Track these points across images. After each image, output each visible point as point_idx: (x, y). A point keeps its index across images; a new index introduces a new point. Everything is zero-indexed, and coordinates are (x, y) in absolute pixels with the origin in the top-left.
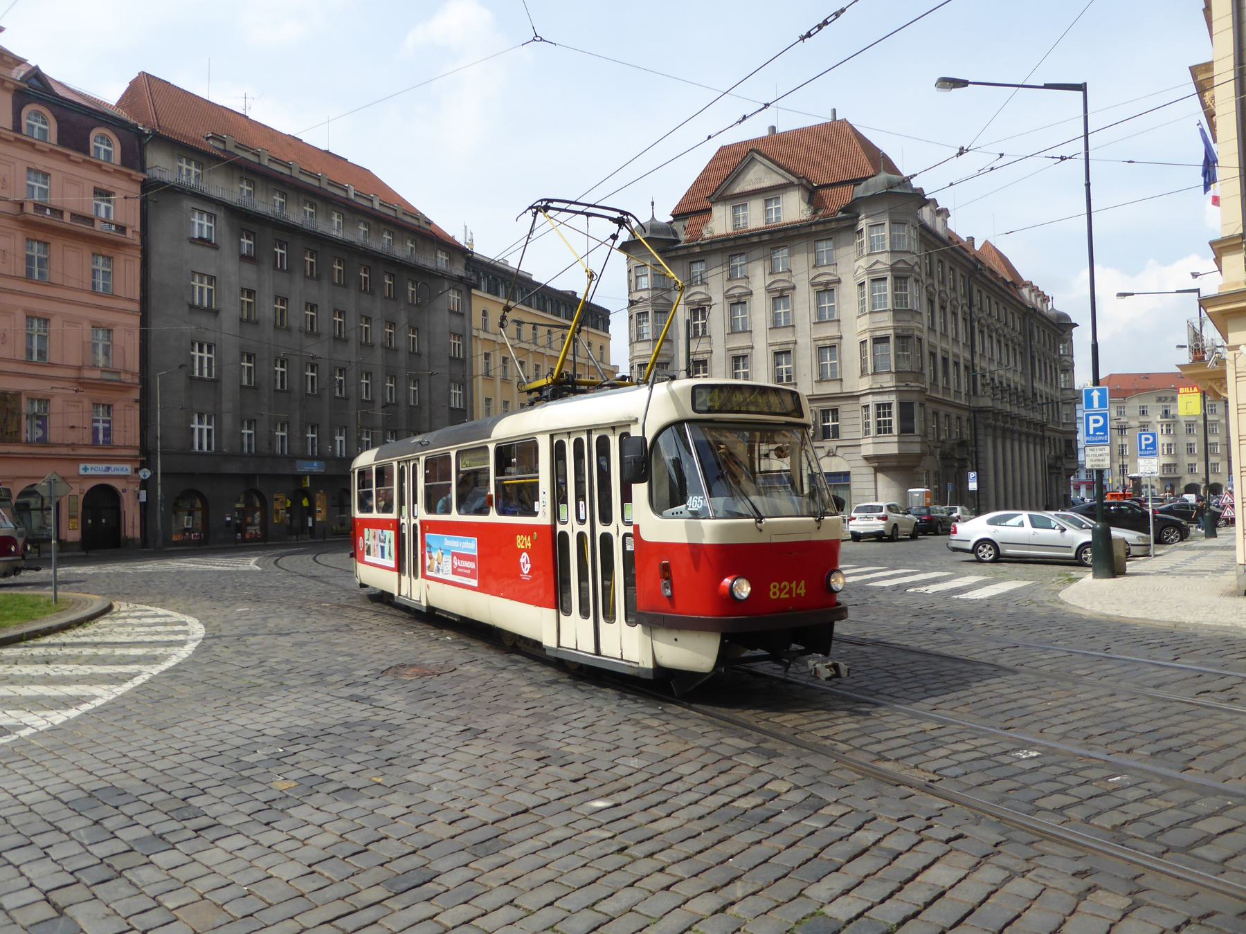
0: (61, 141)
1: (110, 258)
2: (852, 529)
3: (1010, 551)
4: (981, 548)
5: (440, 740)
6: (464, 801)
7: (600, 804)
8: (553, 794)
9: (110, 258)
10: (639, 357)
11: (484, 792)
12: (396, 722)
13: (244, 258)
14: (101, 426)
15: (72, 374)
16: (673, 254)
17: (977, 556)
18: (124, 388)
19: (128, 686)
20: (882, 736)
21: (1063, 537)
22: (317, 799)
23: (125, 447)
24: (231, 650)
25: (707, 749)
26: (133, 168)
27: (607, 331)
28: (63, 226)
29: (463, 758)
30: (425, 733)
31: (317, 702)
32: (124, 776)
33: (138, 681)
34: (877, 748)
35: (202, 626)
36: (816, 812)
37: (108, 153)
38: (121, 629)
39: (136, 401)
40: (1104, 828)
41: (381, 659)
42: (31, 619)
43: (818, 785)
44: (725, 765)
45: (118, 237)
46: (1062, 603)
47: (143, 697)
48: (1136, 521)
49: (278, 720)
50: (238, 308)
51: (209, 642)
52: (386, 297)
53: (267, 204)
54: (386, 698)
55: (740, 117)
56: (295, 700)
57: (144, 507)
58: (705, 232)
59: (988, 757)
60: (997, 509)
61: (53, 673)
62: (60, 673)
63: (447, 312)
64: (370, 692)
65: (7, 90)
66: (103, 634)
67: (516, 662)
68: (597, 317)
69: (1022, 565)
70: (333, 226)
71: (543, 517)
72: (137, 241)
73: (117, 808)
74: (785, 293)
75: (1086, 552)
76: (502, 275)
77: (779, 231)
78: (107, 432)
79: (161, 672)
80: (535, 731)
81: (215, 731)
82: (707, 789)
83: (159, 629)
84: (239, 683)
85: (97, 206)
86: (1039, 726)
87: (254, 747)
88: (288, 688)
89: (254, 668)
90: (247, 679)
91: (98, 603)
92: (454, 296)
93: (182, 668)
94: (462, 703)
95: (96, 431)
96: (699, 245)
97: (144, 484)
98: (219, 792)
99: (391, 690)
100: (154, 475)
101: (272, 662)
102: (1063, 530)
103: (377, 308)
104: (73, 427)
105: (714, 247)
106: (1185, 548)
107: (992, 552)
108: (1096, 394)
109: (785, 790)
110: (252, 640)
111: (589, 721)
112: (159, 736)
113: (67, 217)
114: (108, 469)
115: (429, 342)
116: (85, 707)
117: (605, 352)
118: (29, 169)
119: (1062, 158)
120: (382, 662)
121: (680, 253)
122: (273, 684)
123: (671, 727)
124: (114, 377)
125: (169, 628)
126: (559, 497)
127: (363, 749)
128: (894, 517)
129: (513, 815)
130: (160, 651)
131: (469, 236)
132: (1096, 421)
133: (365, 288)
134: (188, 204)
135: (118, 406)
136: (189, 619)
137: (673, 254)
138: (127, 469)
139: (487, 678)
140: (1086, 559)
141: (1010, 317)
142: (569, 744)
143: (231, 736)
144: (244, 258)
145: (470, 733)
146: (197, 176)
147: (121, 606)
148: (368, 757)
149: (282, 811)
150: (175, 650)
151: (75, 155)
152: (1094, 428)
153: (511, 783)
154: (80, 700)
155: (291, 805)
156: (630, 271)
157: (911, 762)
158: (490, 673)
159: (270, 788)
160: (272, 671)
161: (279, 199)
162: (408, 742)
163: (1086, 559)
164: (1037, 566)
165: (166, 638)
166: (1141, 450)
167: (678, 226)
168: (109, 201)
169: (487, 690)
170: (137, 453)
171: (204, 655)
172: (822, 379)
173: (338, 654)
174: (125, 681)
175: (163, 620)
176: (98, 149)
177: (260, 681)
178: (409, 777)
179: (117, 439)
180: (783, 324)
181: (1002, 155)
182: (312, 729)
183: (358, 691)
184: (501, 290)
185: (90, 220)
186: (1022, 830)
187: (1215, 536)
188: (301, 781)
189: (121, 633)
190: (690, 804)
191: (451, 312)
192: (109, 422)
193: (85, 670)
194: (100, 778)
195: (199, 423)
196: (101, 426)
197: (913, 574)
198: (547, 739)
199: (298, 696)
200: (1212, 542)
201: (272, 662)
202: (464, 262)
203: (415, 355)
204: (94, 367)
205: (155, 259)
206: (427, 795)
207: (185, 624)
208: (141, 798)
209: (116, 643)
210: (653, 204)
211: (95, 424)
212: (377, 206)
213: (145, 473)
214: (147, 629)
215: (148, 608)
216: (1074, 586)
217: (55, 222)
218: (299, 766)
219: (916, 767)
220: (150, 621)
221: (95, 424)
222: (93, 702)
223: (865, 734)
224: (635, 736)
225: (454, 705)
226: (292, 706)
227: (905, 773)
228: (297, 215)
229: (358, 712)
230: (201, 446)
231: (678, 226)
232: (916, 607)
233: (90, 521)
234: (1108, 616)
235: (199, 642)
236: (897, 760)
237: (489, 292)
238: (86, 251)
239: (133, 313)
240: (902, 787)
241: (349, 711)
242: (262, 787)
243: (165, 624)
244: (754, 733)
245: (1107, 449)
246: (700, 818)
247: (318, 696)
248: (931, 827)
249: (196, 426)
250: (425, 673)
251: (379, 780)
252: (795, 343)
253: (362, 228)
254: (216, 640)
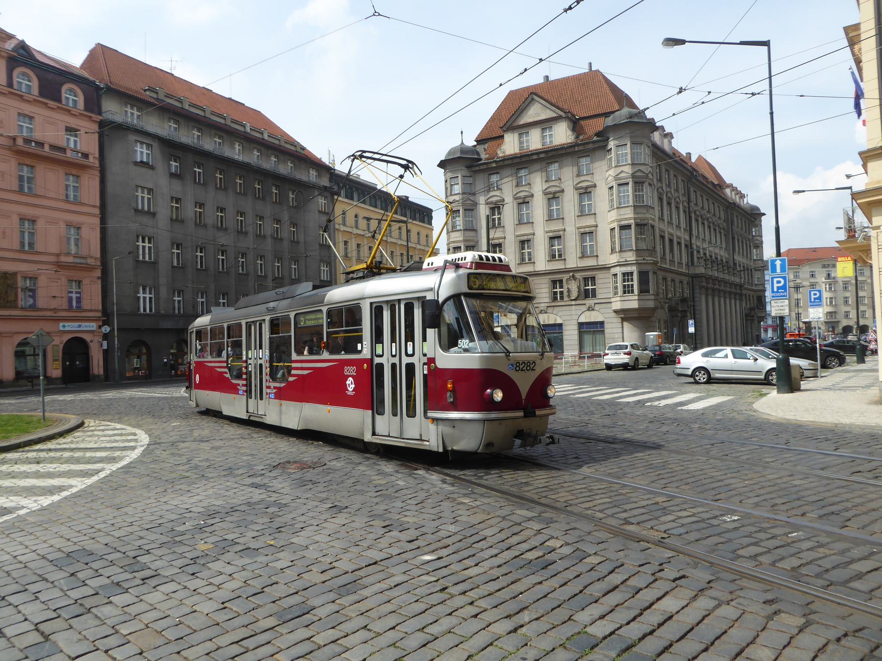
0: (41, 94)
1: (78, 177)
2: (606, 361)
3: (718, 375)
4: (697, 373)
5: (315, 514)
6: (332, 557)
7: (427, 558)
8: (394, 551)
9: (78, 177)
10: (454, 242)
11: (346, 550)
12: (283, 502)
13: (173, 175)
14: (74, 296)
15: (52, 259)
16: (477, 168)
17: (695, 379)
18: (90, 268)
19: (95, 478)
20: (627, 507)
21: (756, 364)
22: (228, 557)
23: (91, 311)
24: (167, 452)
25: (504, 518)
26: (92, 112)
27: (431, 225)
28: (44, 154)
29: (331, 526)
30: (304, 509)
31: (227, 489)
32: (92, 541)
33: (102, 475)
34: (624, 515)
35: (147, 436)
36: (581, 561)
37: (75, 102)
38: (90, 439)
39: (99, 278)
40: (786, 569)
41: (272, 458)
42: (27, 432)
43: (583, 542)
44: (517, 529)
45: (84, 161)
46: (755, 411)
47: (105, 486)
48: (808, 352)
49: (201, 501)
50: (169, 211)
51: (152, 447)
52: (273, 202)
53: (188, 136)
54: (276, 484)
55: (522, 70)
56: (212, 487)
57: (106, 352)
58: (499, 152)
59: (703, 521)
60: (709, 346)
61: (42, 470)
62: (46, 470)
63: (317, 212)
64: (265, 481)
65: (2, 57)
66: (77, 442)
67: (368, 459)
68: (424, 214)
69: (727, 385)
70: (235, 152)
71: (366, 353)
72: (97, 164)
73: (87, 564)
74: (557, 195)
75: (772, 375)
76: (355, 185)
77: (552, 151)
78: (79, 300)
79: (119, 469)
80: (383, 507)
81: (156, 509)
82: (504, 545)
83: (117, 438)
84: (174, 475)
85: (68, 140)
86: (738, 498)
87: (184, 520)
88: (207, 479)
89: (183, 465)
90: (179, 473)
91: (74, 420)
92: (321, 201)
93: (132, 465)
94: (330, 487)
95: (70, 299)
96: (495, 162)
97: (105, 337)
98: (159, 552)
99: (280, 479)
100: (112, 330)
101: (196, 461)
102: (756, 360)
103: (267, 210)
105: (506, 163)
106: (843, 371)
107: (705, 376)
108: (778, 263)
109: (559, 546)
110: (183, 445)
111: (419, 499)
112: (117, 513)
113: (47, 148)
115: (304, 234)
116: (65, 494)
117: (429, 239)
118: (19, 114)
119: (753, 94)
120: (274, 460)
121: (482, 167)
122: (197, 476)
123: (478, 503)
124: (83, 261)
125: (124, 438)
126: (378, 337)
127: (261, 521)
128: (636, 353)
129: (366, 566)
130: (117, 454)
131: (332, 158)
132: (779, 282)
133: (259, 196)
134: (132, 137)
135: (86, 282)
136: (138, 431)
137: (477, 168)
138: (93, 326)
139: (348, 470)
140: (772, 380)
141: (700, 199)
142: (406, 516)
143: (168, 513)
144: (173, 175)
145: (337, 509)
146: (138, 117)
147: (90, 423)
148: (264, 527)
149: (203, 565)
150: (129, 452)
151: (51, 103)
152: (778, 287)
153: (365, 544)
154: (61, 489)
155: (209, 561)
156: (446, 181)
157: (648, 525)
158: (350, 467)
159: (195, 549)
160: (196, 467)
161: (196, 133)
162: (291, 516)
163: (772, 380)
164: (738, 385)
165: (122, 445)
166: (811, 302)
167: (480, 149)
168: (76, 136)
169: (348, 479)
170: (100, 314)
171: (148, 456)
172: (583, 256)
173: (242, 454)
174: (92, 475)
175: (120, 432)
176: (67, 98)
177: (187, 474)
178: (293, 541)
179: (86, 305)
180: (555, 217)
181: (709, 92)
182: (224, 508)
183: (257, 480)
184: (355, 196)
185: (63, 150)
186: (727, 572)
187: (863, 362)
188: (217, 544)
189: (91, 442)
190: (492, 557)
191: (320, 212)
192: (79, 293)
193: (65, 467)
194: (75, 543)
195: (143, 293)
196: (74, 296)
197: (626, 391)
198: (390, 512)
199: (215, 484)
200: (862, 366)
201: (196, 461)
202: (328, 176)
203: (295, 243)
204: (68, 254)
205: (110, 178)
206: (305, 553)
207: (135, 434)
208: (104, 557)
209: (87, 448)
210: (462, 132)
211: (70, 295)
212: (266, 137)
213: (106, 329)
214: (108, 438)
215: (109, 423)
216: (764, 399)
217: (39, 151)
218: (215, 533)
219: (652, 528)
220: (110, 432)
222: (70, 490)
223: (615, 506)
224: (454, 509)
225: (326, 489)
226: (210, 492)
227: (645, 533)
228: (210, 144)
229: (257, 495)
230: (145, 310)
231: (480, 149)
232: (651, 416)
233: (68, 363)
234: (788, 420)
235: (145, 447)
236: (638, 523)
237: (346, 197)
238: (61, 172)
239: (94, 215)
240: (642, 543)
241: (251, 494)
242: (190, 549)
243: (121, 435)
244: (537, 506)
245: (787, 302)
246: (499, 566)
247: (229, 484)
248: (663, 570)
249: (141, 295)
250: (303, 466)
251: (272, 543)
252: (564, 230)
253: (256, 153)
254: (157, 446)
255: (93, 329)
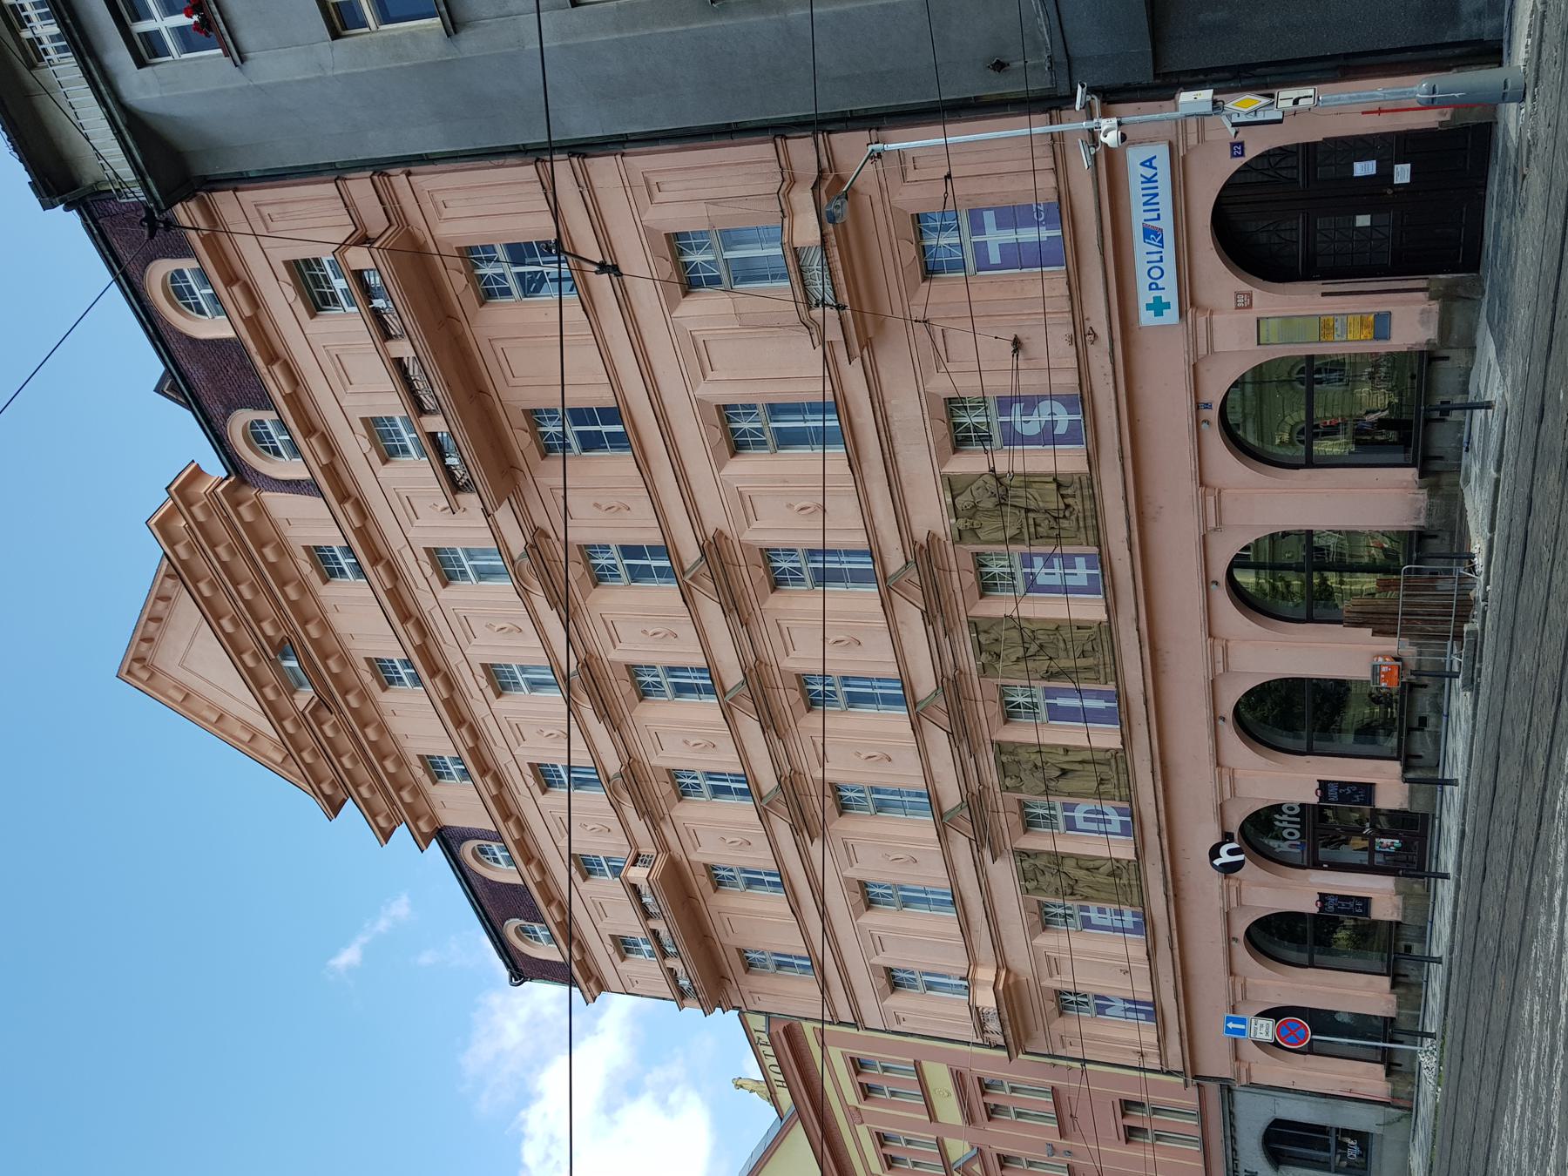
14: (996, 238)
104: (1017, 344)
114: (1151, 233)
135: (916, 196)
211: (995, 258)
221: (995, 258)
255: (1163, 164)
